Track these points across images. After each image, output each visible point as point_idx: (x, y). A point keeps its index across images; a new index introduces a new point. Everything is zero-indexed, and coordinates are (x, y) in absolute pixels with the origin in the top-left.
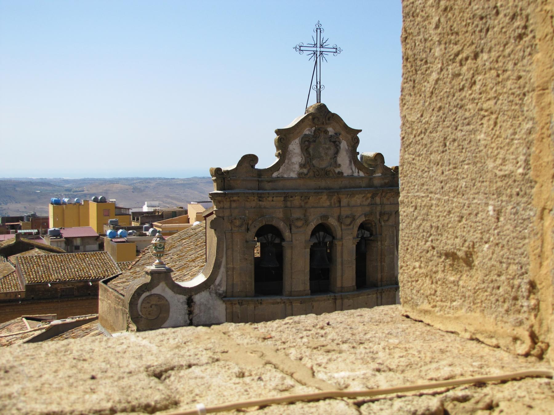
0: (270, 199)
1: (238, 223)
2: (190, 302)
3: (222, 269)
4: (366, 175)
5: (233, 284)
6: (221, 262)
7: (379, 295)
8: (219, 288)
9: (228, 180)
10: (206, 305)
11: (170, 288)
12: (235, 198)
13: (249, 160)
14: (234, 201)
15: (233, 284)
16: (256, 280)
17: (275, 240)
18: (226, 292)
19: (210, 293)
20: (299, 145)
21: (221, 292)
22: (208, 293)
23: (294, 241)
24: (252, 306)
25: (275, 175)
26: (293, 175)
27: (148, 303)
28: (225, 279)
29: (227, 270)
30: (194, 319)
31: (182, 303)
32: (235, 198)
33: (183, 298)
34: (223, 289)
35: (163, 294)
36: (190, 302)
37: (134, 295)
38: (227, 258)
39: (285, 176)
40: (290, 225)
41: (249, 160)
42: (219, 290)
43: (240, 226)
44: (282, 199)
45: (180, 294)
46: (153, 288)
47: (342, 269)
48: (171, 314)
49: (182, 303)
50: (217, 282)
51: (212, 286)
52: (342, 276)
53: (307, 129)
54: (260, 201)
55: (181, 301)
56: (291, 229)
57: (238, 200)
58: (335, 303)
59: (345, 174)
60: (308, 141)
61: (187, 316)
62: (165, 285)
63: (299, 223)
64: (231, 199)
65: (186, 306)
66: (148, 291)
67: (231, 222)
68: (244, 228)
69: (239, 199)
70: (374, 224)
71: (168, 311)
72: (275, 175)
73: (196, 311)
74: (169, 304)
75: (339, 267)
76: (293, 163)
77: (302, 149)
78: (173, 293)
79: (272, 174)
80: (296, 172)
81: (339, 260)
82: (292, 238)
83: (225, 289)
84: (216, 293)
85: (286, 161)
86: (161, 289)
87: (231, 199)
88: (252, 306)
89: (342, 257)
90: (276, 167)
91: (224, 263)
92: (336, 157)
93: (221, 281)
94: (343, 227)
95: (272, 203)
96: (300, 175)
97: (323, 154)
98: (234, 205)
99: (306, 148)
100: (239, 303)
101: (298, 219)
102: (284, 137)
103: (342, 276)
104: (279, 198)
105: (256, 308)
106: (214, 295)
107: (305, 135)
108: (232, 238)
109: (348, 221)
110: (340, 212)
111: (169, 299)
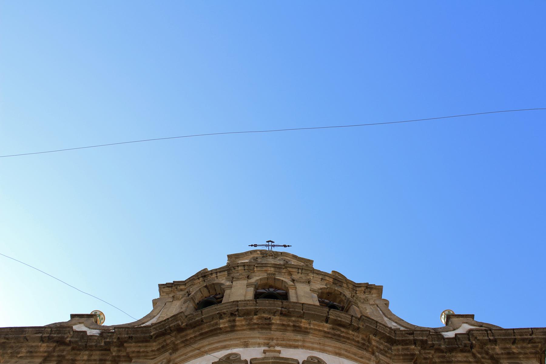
44: (226, 273)
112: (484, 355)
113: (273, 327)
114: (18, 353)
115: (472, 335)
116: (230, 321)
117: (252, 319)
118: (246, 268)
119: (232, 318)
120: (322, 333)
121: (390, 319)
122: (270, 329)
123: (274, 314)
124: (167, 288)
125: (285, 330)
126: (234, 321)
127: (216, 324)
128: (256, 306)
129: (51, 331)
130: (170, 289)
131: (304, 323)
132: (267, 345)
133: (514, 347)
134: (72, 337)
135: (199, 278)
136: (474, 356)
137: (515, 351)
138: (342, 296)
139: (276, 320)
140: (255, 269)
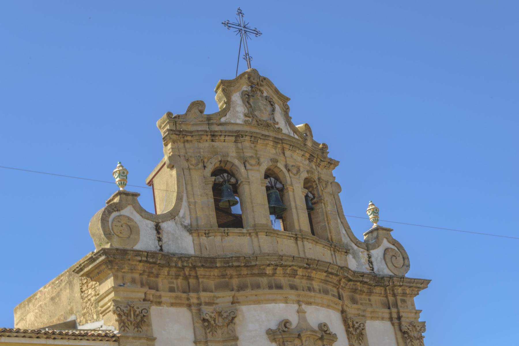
0: (222, 138)
1: (194, 161)
2: (158, 229)
3: (184, 204)
4: (300, 139)
5: (197, 218)
6: (182, 196)
7: (333, 252)
8: (183, 220)
9: (180, 124)
10: (173, 234)
11: (138, 212)
12: (189, 138)
13: (198, 105)
14: (187, 141)
15: (197, 218)
16: (217, 218)
17: (231, 178)
18: (191, 225)
19: (176, 223)
20: (240, 98)
21: (186, 224)
22: (174, 224)
23: (250, 177)
24: (218, 238)
25: (223, 120)
26: (239, 121)
27: (119, 221)
28: (188, 213)
29: (189, 204)
30: (163, 246)
31: (151, 228)
32: (189, 138)
33: (151, 224)
34: (187, 222)
35: (131, 217)
36: (158, 229)
37: (104, 212)
38: (187, 193)
39: (232, 122)
40: (244, 163)
41: (198, 105)
42: (184, 222)
43: (197, 164)
44: (233, 139)
45: (148, 219)
46: (122, 209)
47: (298, 214)
48: (141, 237)
49: (151, 228)
50: (181, 214)
51: (176, 217)
52: (298, 220)
53: (245, 86)
54: (212, 141)
55: (150, 226)
56: (245, 167)
57: (191, 141)
58: (297, 243)
59: (283, 132)
60: (248, 95)
61: (157, 242)
62: (132, 209)
63: (253, 162)
64: (186, 138)
65: (155, 232)
66: (117, 210)
67: (187, 160)
68: (201, 165)
69: (192, 139)
70: (315, 186)
71: (138, 233)
72: (223, 120)
73: (165, 239)
74: (138, 227)
75: (294, 211)
76: (237, 112)
77: (243, 101)
78: (140, 217)
79: (221, 118)
80: (241, 120)
81: (293, 204)
82: (248, 175)
83: (189, 222)
84: (182, 224)
85: (231, 109)
86: (128, 211)
87: (186, 138)
88: (218, 238)
89: (295, 202)
90: (224, 112)
91: (185, 198)
92: (273, 114)
93: (184, 214)
94: (291, 175)
95: (224, 144)
96: (245, 121)
97: (262, 108)
98: (187, 145)
99: (247, 100)
100: (205, 234)
101: (251, 157)
102: (227, 87)
103: (298, 220)
104: (230, 138)
105: (223, 240)
106: (180, 226)
107: (244, 91)
108: (190, 175)
109: (295, 171)
110: (286, 162)
111: (138, 223)
112: (391, 292)
113: (297, 277)
114: (122, 269)
115: (393, 280)
116: (273, 269)
117: (287, 269)
118: (252, 139)
119: (275, 267)
120: (320, 280)
121: (342, 223)
122: (295, 277)
123: (300, 267)
124: (175, 135)
125: (303, 278)
126: (276, 269)
127: (264, 269)
128: (292, 261)
129: (147, 255)
130: (177, 136)
131: (313, 274)
132: (299, 302)
133: (408, 289)
134: (160, 259)
135: (207, 135)
136: (386, 290)
137: (408, 292)
138: (314, 184)
139: (300, 272)
140: (259, 141)
